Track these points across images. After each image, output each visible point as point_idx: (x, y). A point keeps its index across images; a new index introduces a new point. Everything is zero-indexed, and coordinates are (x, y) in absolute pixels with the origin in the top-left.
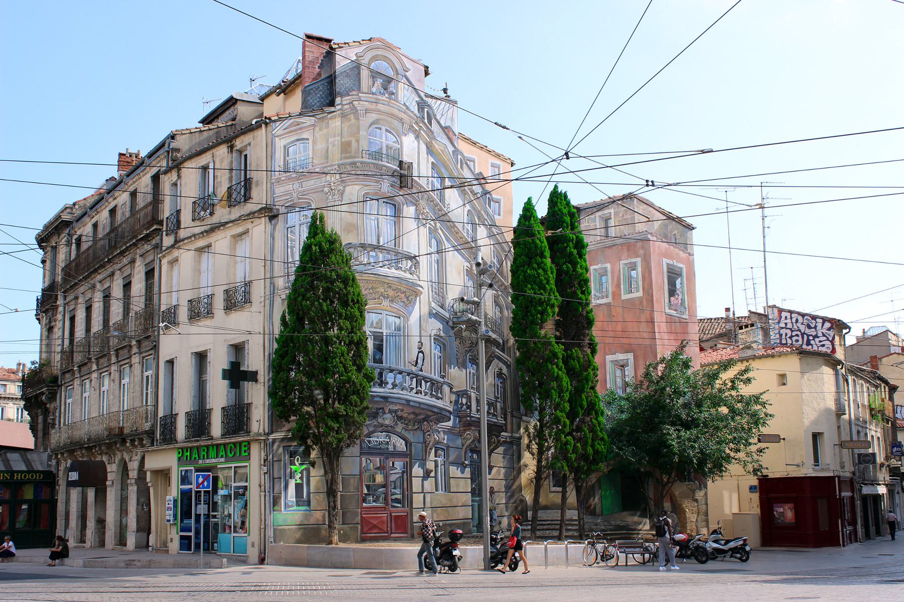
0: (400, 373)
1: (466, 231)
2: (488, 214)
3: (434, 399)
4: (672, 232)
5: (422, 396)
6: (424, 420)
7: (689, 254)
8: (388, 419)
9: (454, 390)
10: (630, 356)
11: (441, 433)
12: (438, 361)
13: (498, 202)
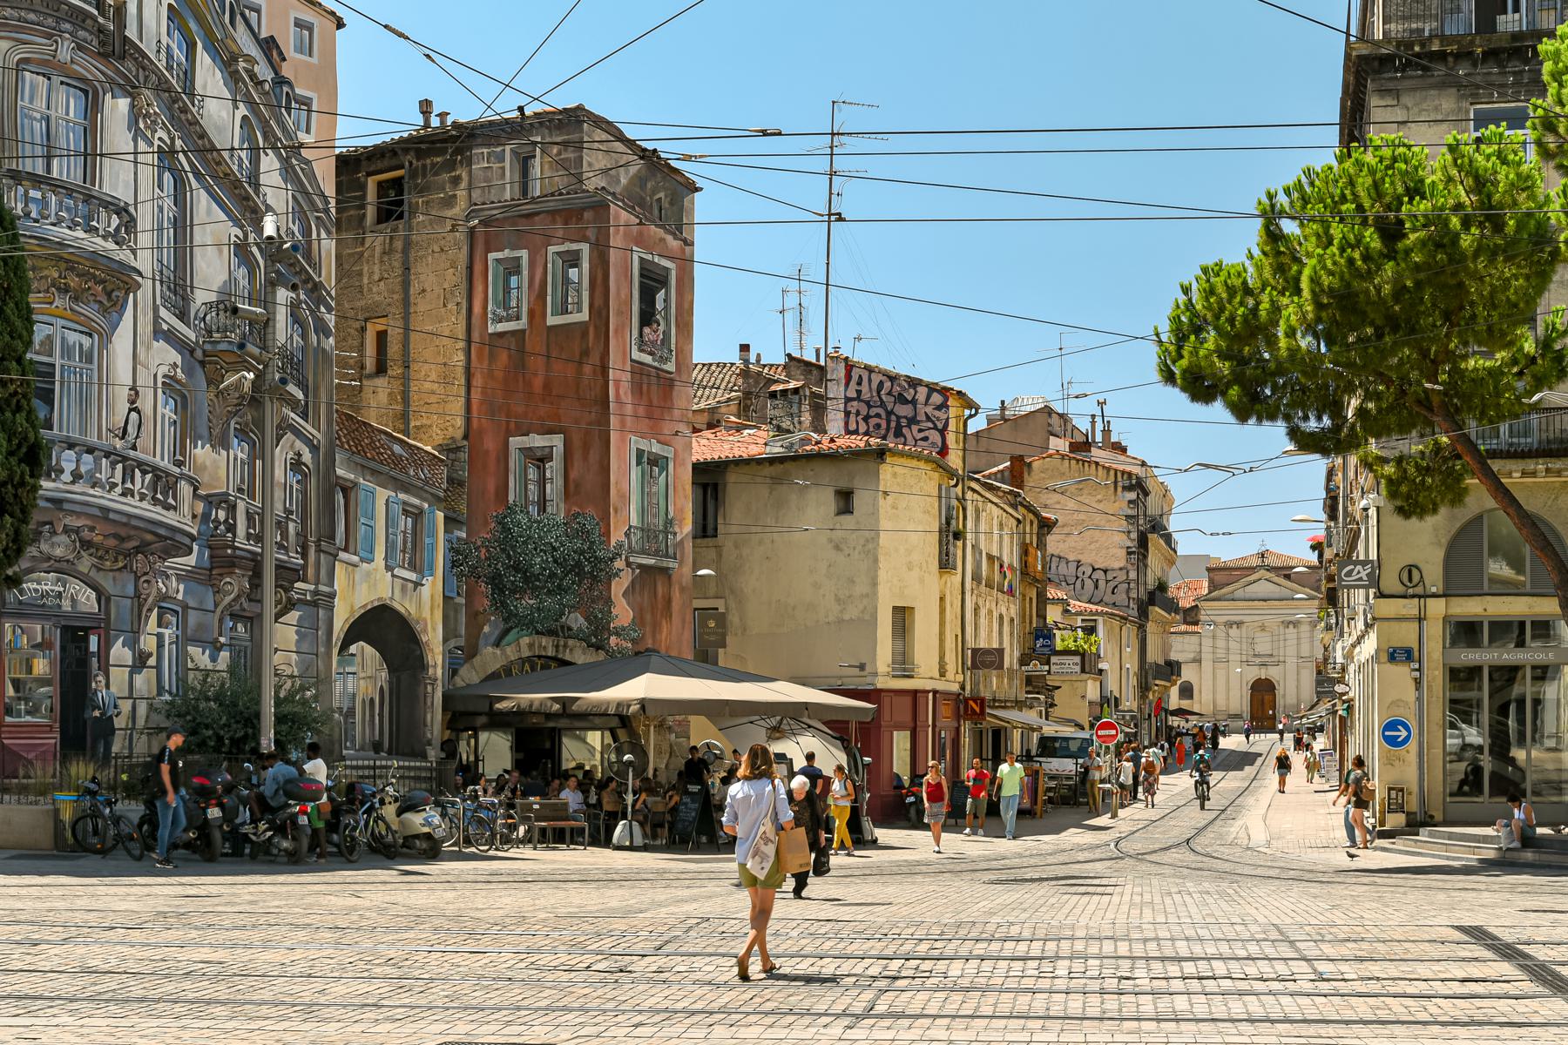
0: (90, 451)
1: (238, 163)
2: (284, 129)
3: (159, 509)
4: (654, 194)
5: (135, 501)
6: (138, 550)
8: (60, 547)
9: (201, 492)
10: (557, 441)
11: (173, 577)
12: (169, 431)
13: (306, 102)
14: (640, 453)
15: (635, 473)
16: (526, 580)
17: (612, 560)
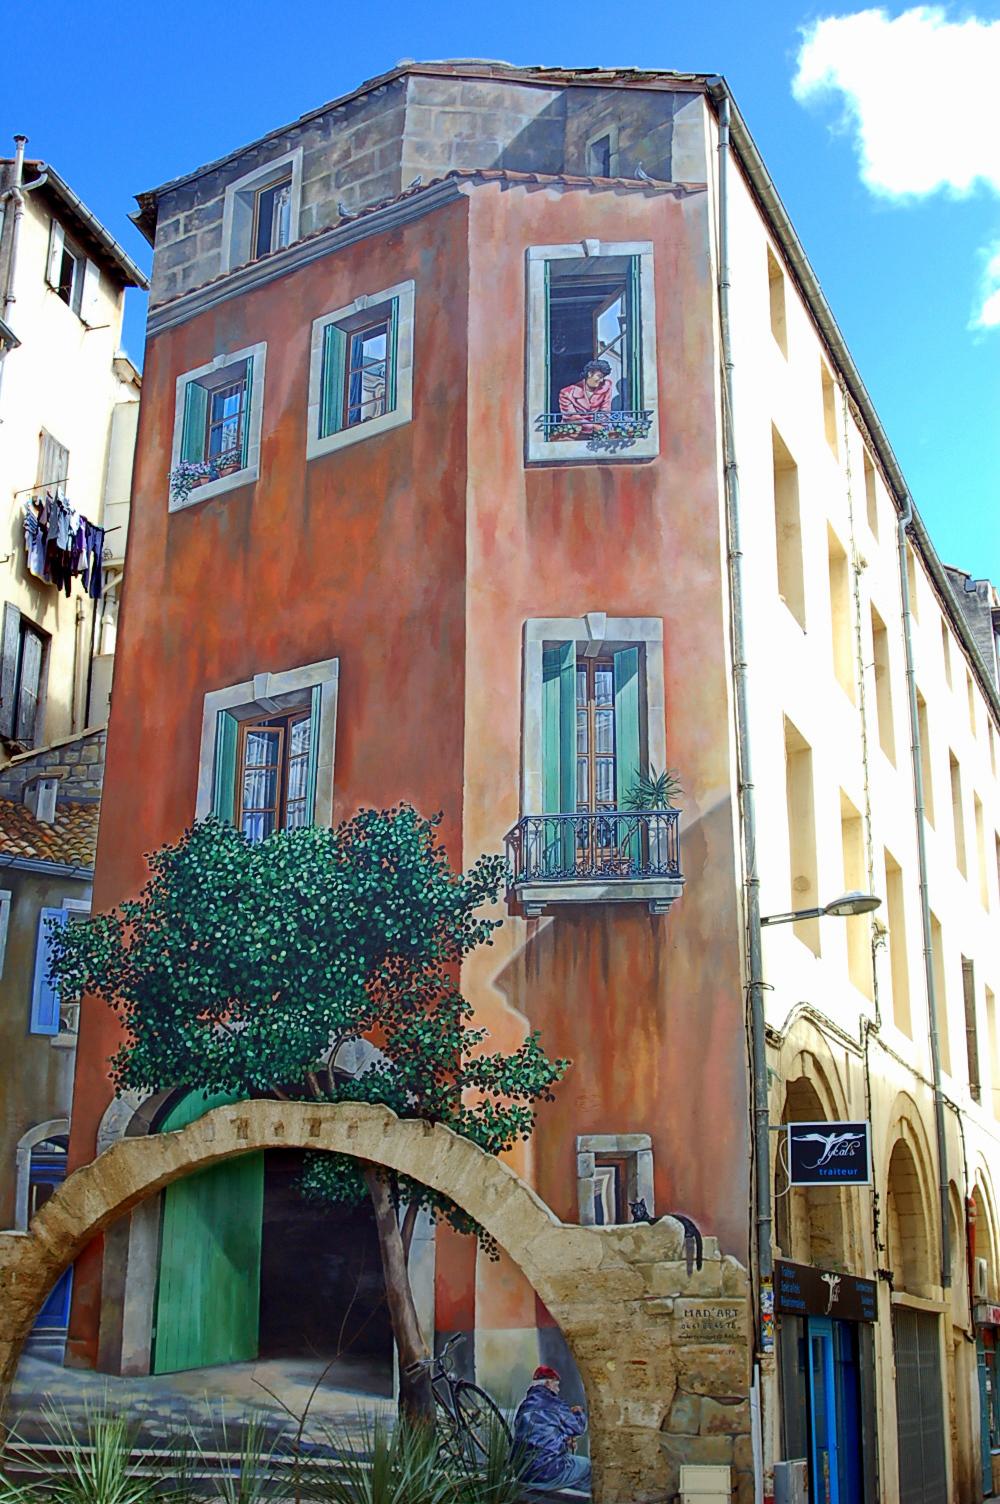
7: (680, 191)
10: (324, 677)
14: (553, 659)
15: (540, 697)
16: (227, 978)
17: (464, 905)
